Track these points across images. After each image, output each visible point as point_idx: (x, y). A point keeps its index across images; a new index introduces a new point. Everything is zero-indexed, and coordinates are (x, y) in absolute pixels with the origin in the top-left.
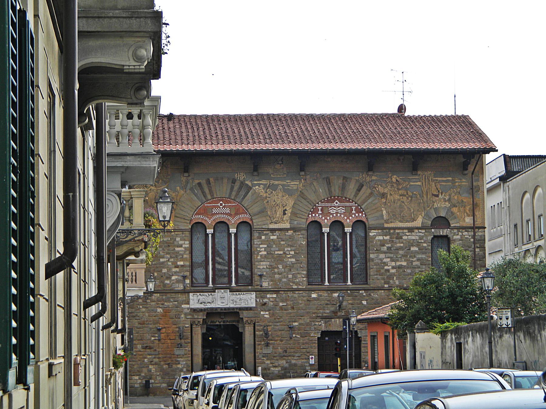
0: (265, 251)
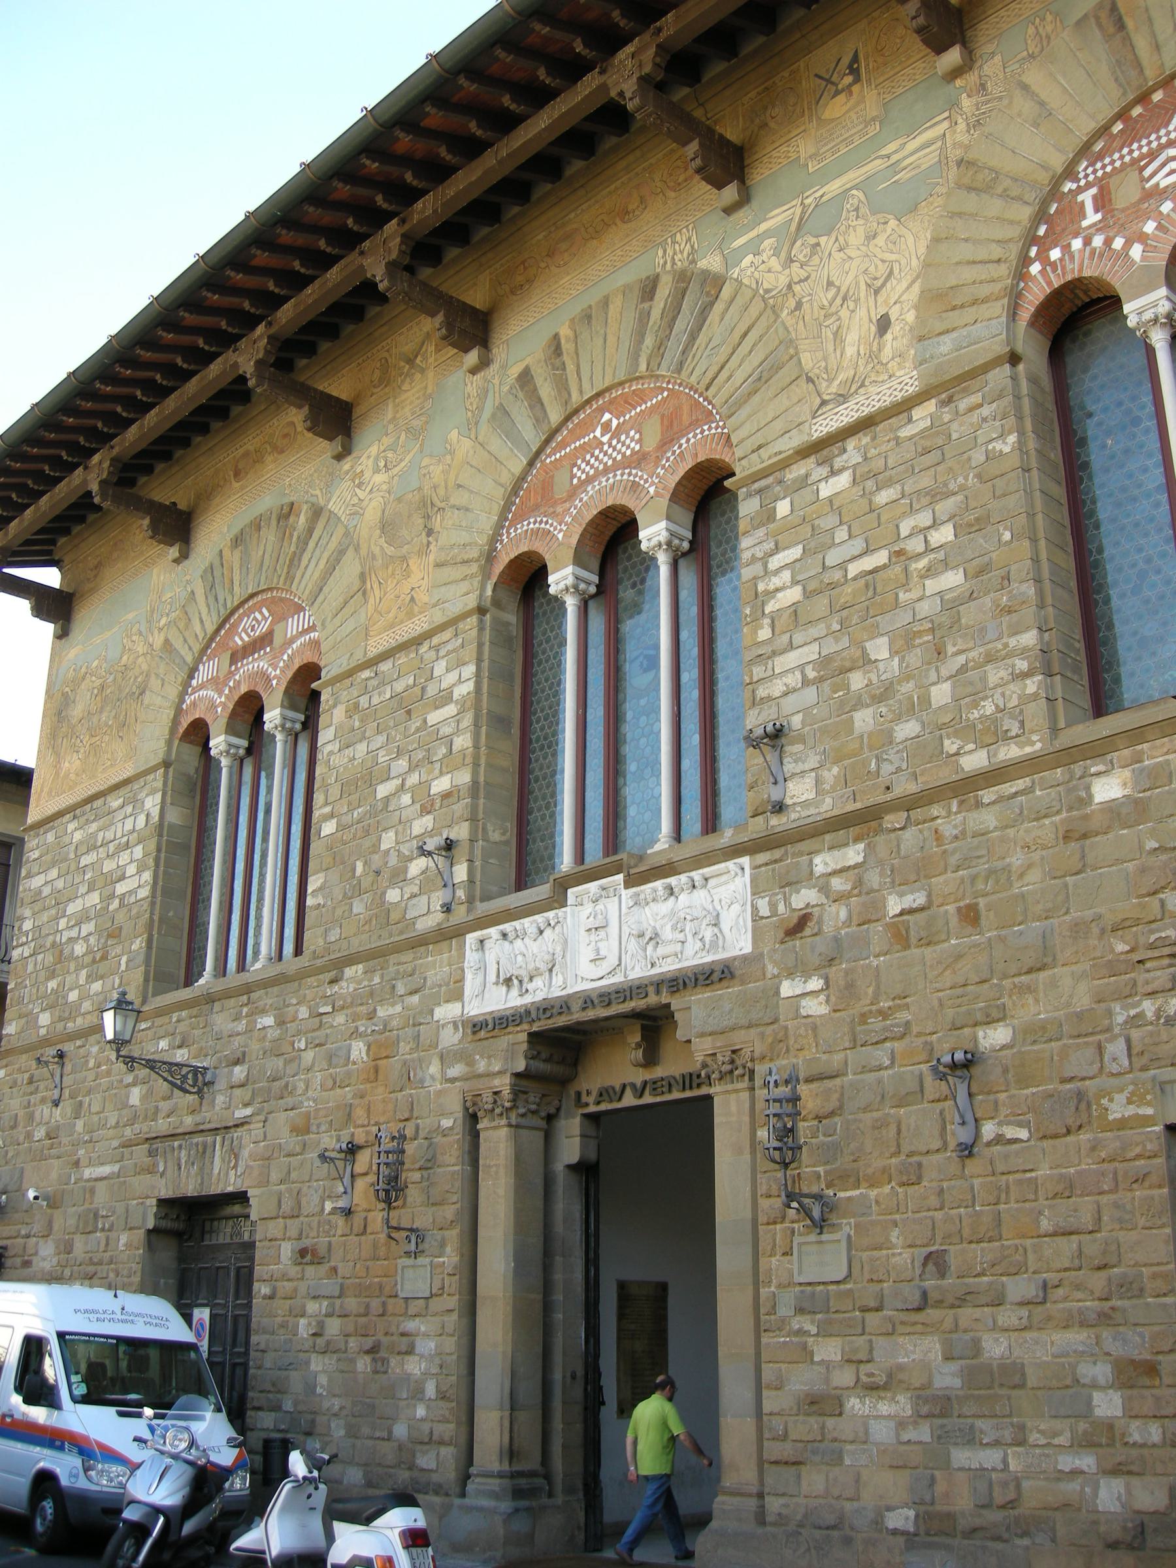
0: (795, 582)
